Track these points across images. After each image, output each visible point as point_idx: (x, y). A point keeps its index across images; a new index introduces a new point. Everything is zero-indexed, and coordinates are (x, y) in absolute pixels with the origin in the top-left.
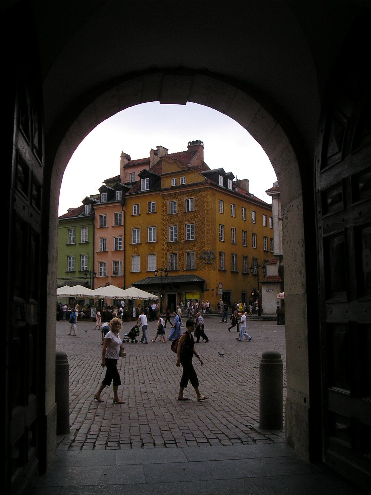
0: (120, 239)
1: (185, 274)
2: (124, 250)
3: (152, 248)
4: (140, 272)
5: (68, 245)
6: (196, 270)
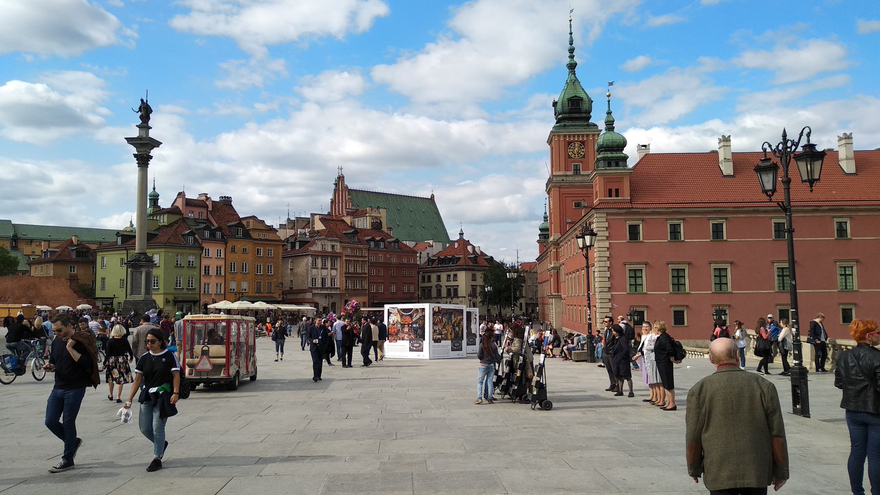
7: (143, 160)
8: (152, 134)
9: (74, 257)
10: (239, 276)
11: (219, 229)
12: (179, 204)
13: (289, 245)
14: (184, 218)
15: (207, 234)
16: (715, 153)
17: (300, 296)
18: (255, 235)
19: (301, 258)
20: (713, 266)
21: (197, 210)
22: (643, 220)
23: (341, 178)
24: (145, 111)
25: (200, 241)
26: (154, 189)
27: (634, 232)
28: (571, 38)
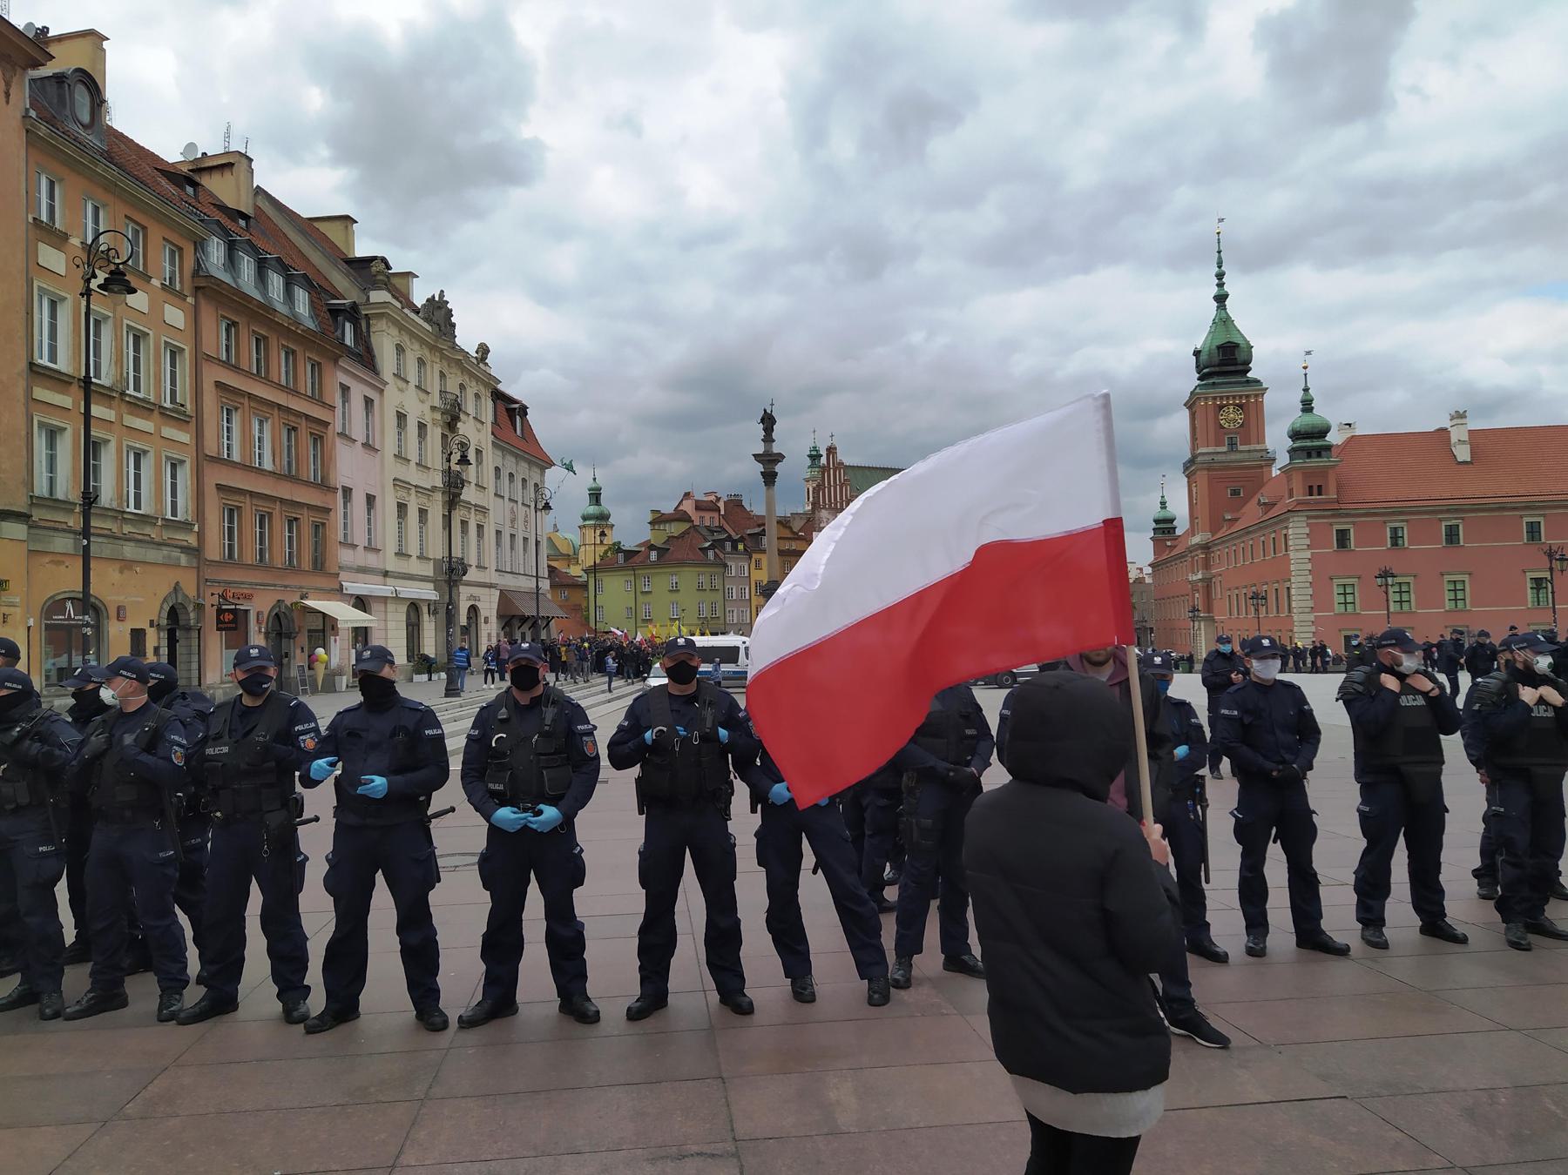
7: (769, 478)
8: (776, 449)
11: (742, 539)
15: (728, 545)
16: (1443, 432)
20: (1447, 578)
21: (708, 515)
22: (1354, 523)
23: (831, 450)
24: (768, 421)
27: (1343, 537)
28: (1220, 258)
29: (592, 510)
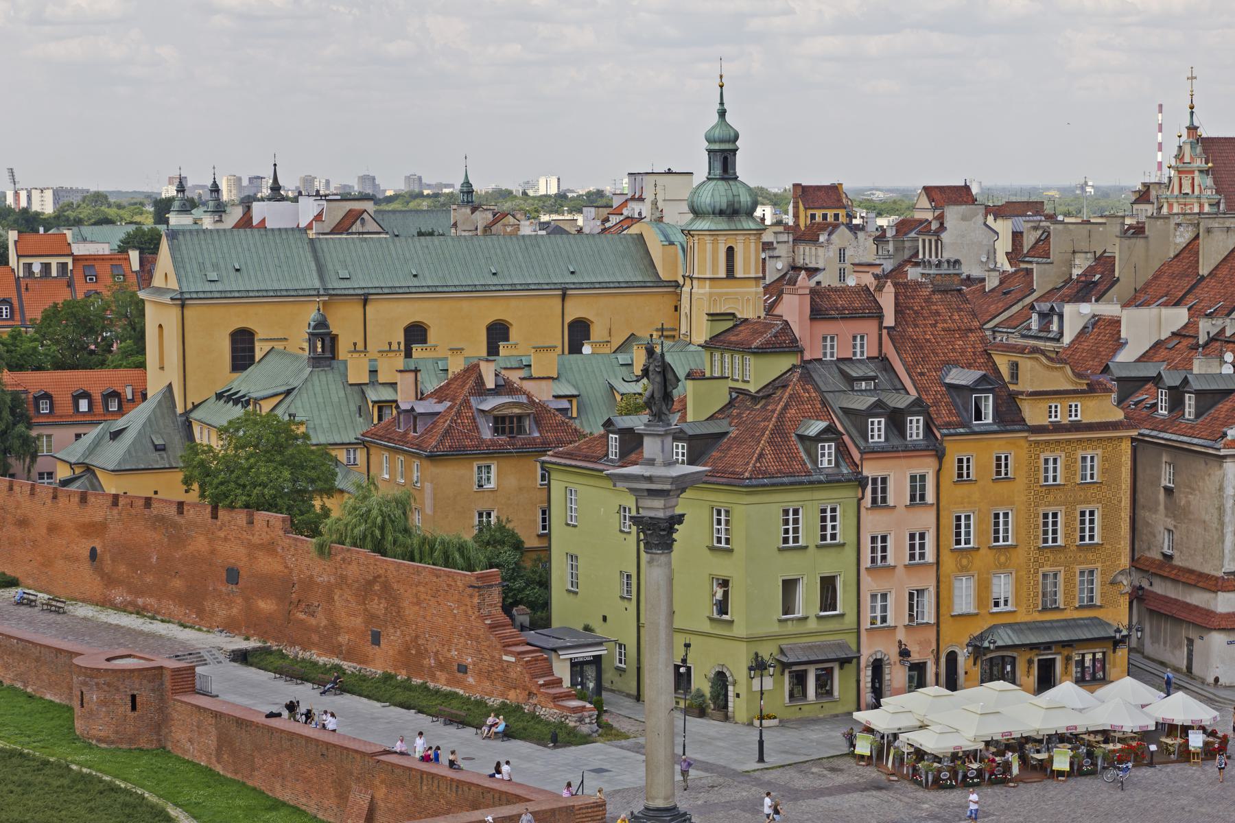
0: (922, 536)
1: (1076, 615)
2: (938, 563)
3: (1003, 559)
4: (977, 614)
5: (780, 550)
6: (1101, 607)
9: (487, 434)
10: (985, 557)
11: (918, 406)
12: (793, 309)
13: (1163, 398)
14: (805, 364)
15: (878, 429)
17: (1197, 598)
18: (1034, 413)
19: (1200, 464)
21: (845, 329)
25: (856, 456)
26: (722, 113)
29: (715, 194)
